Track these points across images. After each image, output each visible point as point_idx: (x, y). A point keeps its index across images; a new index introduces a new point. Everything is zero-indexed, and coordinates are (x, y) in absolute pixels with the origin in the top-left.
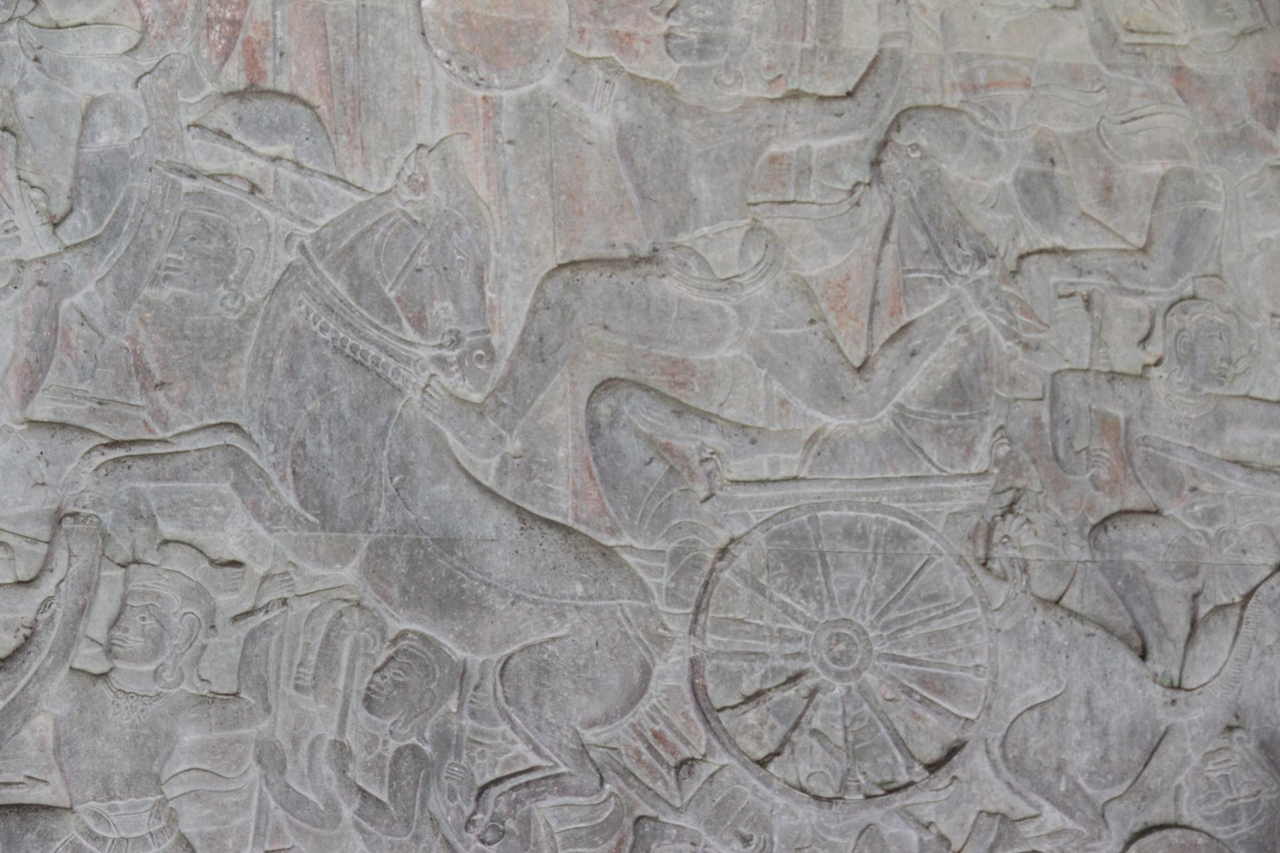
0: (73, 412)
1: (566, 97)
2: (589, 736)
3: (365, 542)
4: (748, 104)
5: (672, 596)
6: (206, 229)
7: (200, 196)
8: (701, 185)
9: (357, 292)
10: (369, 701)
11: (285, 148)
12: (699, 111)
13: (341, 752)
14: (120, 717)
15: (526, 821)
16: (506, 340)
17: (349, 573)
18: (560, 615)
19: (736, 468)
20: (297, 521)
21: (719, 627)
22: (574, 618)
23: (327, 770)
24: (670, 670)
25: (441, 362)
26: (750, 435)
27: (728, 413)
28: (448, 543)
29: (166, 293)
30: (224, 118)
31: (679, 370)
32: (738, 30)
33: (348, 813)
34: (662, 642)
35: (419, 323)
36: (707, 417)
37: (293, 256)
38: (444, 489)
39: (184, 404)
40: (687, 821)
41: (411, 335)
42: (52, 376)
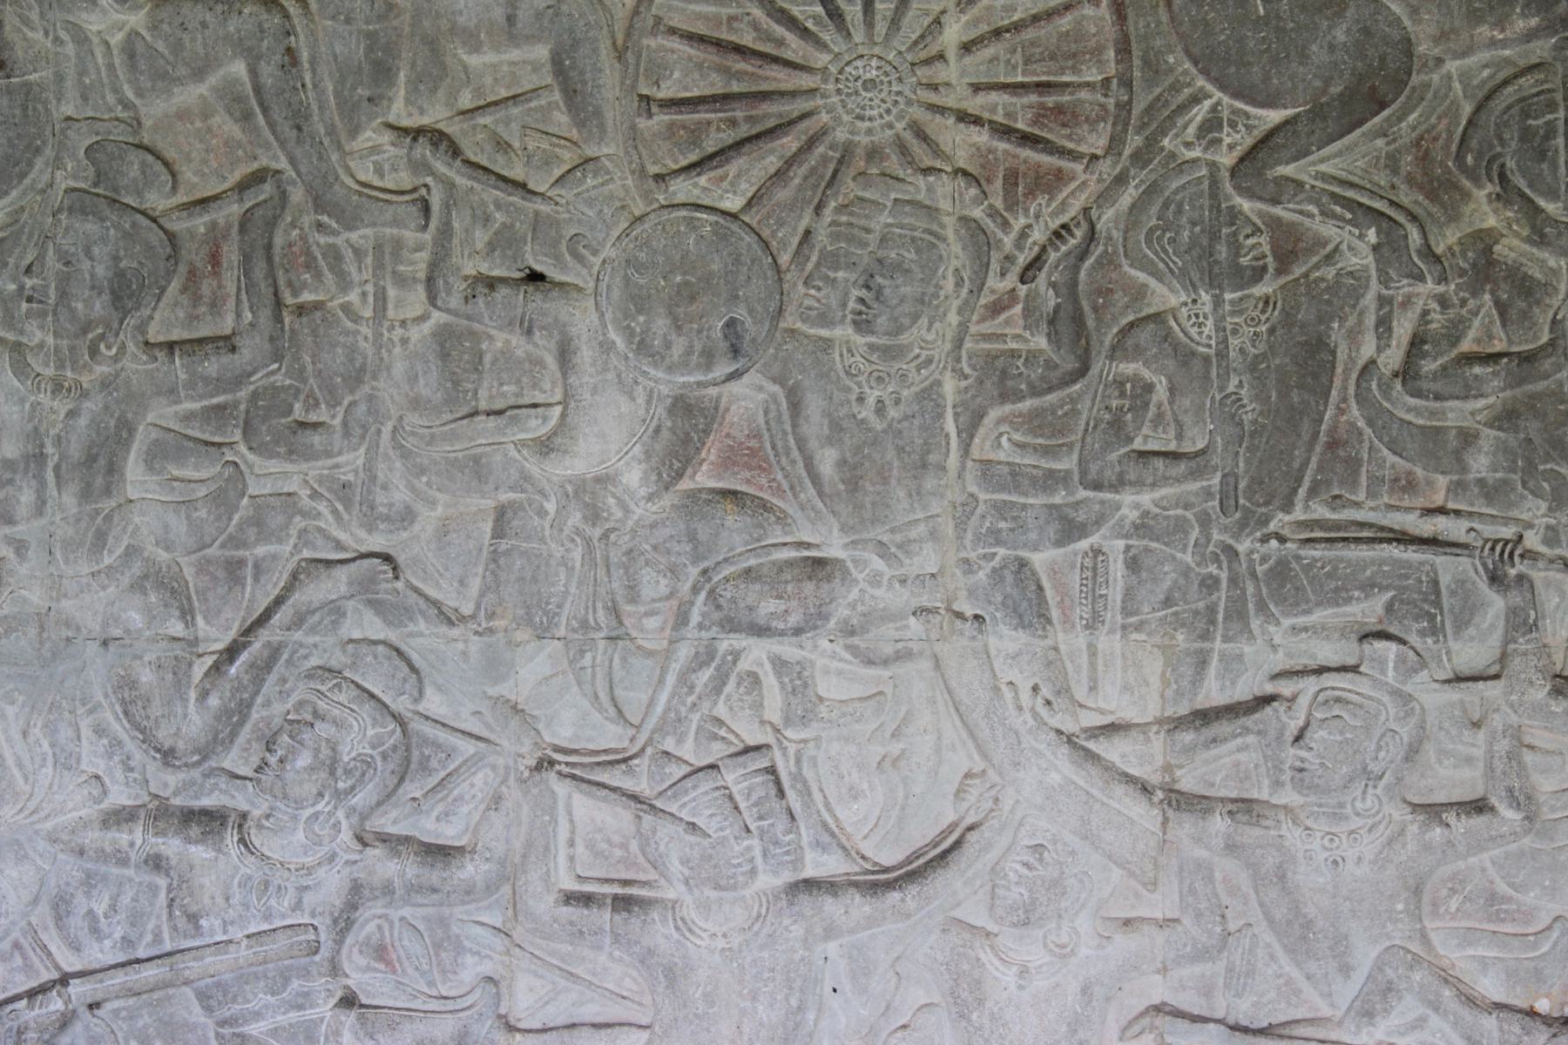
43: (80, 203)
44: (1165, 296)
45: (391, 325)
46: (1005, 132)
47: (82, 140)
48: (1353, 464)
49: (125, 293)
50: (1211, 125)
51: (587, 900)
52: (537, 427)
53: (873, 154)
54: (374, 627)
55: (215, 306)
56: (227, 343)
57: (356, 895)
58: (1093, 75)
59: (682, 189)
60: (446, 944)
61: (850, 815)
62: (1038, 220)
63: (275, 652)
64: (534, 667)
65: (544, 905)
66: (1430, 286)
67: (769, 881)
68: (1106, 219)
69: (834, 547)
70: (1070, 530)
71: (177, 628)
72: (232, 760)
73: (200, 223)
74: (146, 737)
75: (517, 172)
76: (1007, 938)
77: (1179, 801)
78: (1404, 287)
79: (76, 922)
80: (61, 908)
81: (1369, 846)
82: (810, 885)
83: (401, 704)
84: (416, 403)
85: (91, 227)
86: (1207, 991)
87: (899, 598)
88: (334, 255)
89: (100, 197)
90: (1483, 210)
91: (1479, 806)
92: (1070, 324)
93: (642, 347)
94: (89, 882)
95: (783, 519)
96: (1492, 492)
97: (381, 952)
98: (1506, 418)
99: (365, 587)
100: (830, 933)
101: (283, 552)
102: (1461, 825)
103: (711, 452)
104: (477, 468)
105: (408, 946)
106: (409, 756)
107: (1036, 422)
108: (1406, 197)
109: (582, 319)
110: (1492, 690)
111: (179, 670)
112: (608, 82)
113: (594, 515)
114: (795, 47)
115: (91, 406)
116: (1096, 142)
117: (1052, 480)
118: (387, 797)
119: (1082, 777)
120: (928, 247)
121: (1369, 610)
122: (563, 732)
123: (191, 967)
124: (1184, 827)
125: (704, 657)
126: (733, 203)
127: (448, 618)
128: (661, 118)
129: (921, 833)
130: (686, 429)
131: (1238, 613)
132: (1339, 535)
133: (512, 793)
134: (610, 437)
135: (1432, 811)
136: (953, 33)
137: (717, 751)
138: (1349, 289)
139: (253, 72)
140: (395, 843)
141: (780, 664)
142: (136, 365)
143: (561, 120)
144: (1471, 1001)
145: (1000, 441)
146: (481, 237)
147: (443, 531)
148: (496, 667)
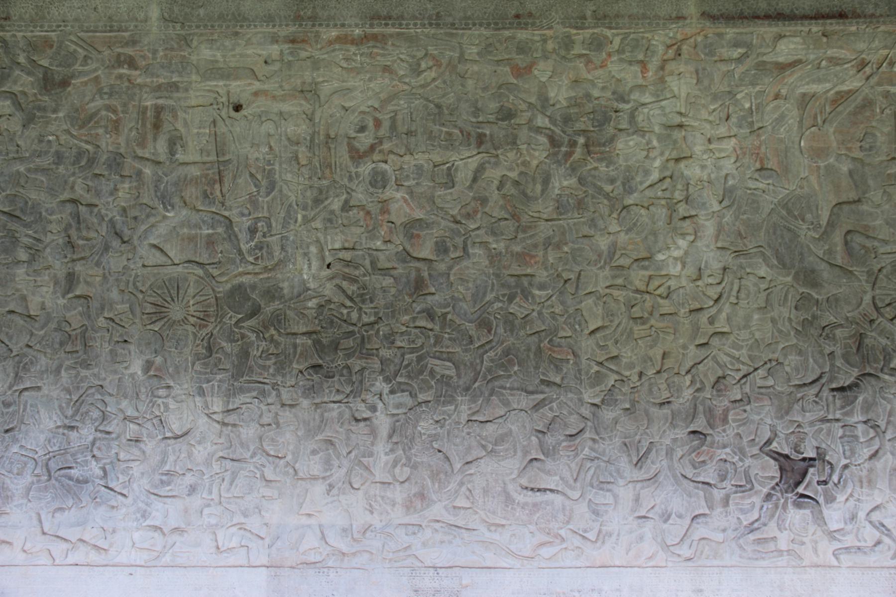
0: (726, 245)
1: (836, 164)
2: (848, 315)
3: (793, 272)
4: (882, 162)
5: (867, 281)
6: (754, 201)
7: (752, 194)
8: (871, 182)
9: (788, 214)
10: (796, 308)
11: (770, 181)
12: (869, 164)
13: (790, 319)
14: (741, 313)
15: (834, 335)
16: (824, 223)
17: (789, 279)
18: (840, 287)
19: (882, 250)
20: (777, 267)
21: (880, 288)
22: (844, 288)
23: (787, 324)
24: (867, 298)
25: (809, 229)
26: (885, 242)
27: (880, 237)
28: (813, 271)
29: (745, 217)
30: (756, 176)
31: (867, 227)
32: (878, 144)
33: (792, 333)
34: (865, 292)
35: (803, 220)
36: (874, 238)
37: (773, 206)
38: (811, 259)
39: (751, 242)
40: (873, 334)
41: (801, 223)
42: (721, 237)
43: (56, 330)
44: (224, 344)
45: (102, 347)
46: (198, 318)
47: (56, 320)
48: (252, 371)
50: (231, 317)
52: (125, 365)
53: (179, 321)
54: (100, 397)
56: (77, 352)
57: (95, 440)
58: (212, 309)
59: (149, 327)
60: (109, 448)
61: (173, 427)
62: (204, 332)
63: (83, 401)
64: (124, 404)
65: (124, 441)
66: (264, 343)
67: (160, 437)
68: (215, 332)
69: (172, 384)
70: (208, 381)
71: (68, 397)
72: (77, 418)
73: (74, 333)
74: (63, 414)
75: (123, 324)
76: (197, 446)
77: (224, 424)
78: (260, 343)
80: (49, 441)
81: (253, 431)
82: (166, 438)
83: (103, 409)
84: (107, 361)
85: (56, 334)
86: (228, 454)
87: (182, 392)
89: (59, 329)
90: (273, 331)
91: (270, 425)
92: (209, 349)
93: (141, 352)
94: (54, 437)
95: (164, 379)
96: (273, 375)
97: (99, 449)
98: (275, 364)
99: (98, 391)
100: (169, 445)
101: (85, 385)
102: (266, 428)
103: (153, 369)
104: (115, 372)
105: (103, 448)
106: (104, 417)
107: (204, 364)
108: (261, 329)
109: (132, 348)
110: (273, 407)
111: (68, 404)
112: (138, 310)
113: (133, 379)
114: (167, 305)
115: (56, 362)
116: (213, 320)
117: (206, 373)
118: (101, 424)
119: (209, 421)
120: (187, 336)
121: (254, 394)
122: (129, 414)
124: (224, 429)
125: (151, 401)
126: (156, 329)
128: (146, 316)
129: (185, 430)
130: (148, 366)
131: (234, 394)
132: (249, 382)
134: (137, 367)
135: (263, 426)
136: (191, 303)
138: (252, 343)
140: (101, 431)
141: (163, 403)
142: (63, 355)
143: (131, 316)
144: (268, 455)
145: (198, 367)
148: (118, 403)
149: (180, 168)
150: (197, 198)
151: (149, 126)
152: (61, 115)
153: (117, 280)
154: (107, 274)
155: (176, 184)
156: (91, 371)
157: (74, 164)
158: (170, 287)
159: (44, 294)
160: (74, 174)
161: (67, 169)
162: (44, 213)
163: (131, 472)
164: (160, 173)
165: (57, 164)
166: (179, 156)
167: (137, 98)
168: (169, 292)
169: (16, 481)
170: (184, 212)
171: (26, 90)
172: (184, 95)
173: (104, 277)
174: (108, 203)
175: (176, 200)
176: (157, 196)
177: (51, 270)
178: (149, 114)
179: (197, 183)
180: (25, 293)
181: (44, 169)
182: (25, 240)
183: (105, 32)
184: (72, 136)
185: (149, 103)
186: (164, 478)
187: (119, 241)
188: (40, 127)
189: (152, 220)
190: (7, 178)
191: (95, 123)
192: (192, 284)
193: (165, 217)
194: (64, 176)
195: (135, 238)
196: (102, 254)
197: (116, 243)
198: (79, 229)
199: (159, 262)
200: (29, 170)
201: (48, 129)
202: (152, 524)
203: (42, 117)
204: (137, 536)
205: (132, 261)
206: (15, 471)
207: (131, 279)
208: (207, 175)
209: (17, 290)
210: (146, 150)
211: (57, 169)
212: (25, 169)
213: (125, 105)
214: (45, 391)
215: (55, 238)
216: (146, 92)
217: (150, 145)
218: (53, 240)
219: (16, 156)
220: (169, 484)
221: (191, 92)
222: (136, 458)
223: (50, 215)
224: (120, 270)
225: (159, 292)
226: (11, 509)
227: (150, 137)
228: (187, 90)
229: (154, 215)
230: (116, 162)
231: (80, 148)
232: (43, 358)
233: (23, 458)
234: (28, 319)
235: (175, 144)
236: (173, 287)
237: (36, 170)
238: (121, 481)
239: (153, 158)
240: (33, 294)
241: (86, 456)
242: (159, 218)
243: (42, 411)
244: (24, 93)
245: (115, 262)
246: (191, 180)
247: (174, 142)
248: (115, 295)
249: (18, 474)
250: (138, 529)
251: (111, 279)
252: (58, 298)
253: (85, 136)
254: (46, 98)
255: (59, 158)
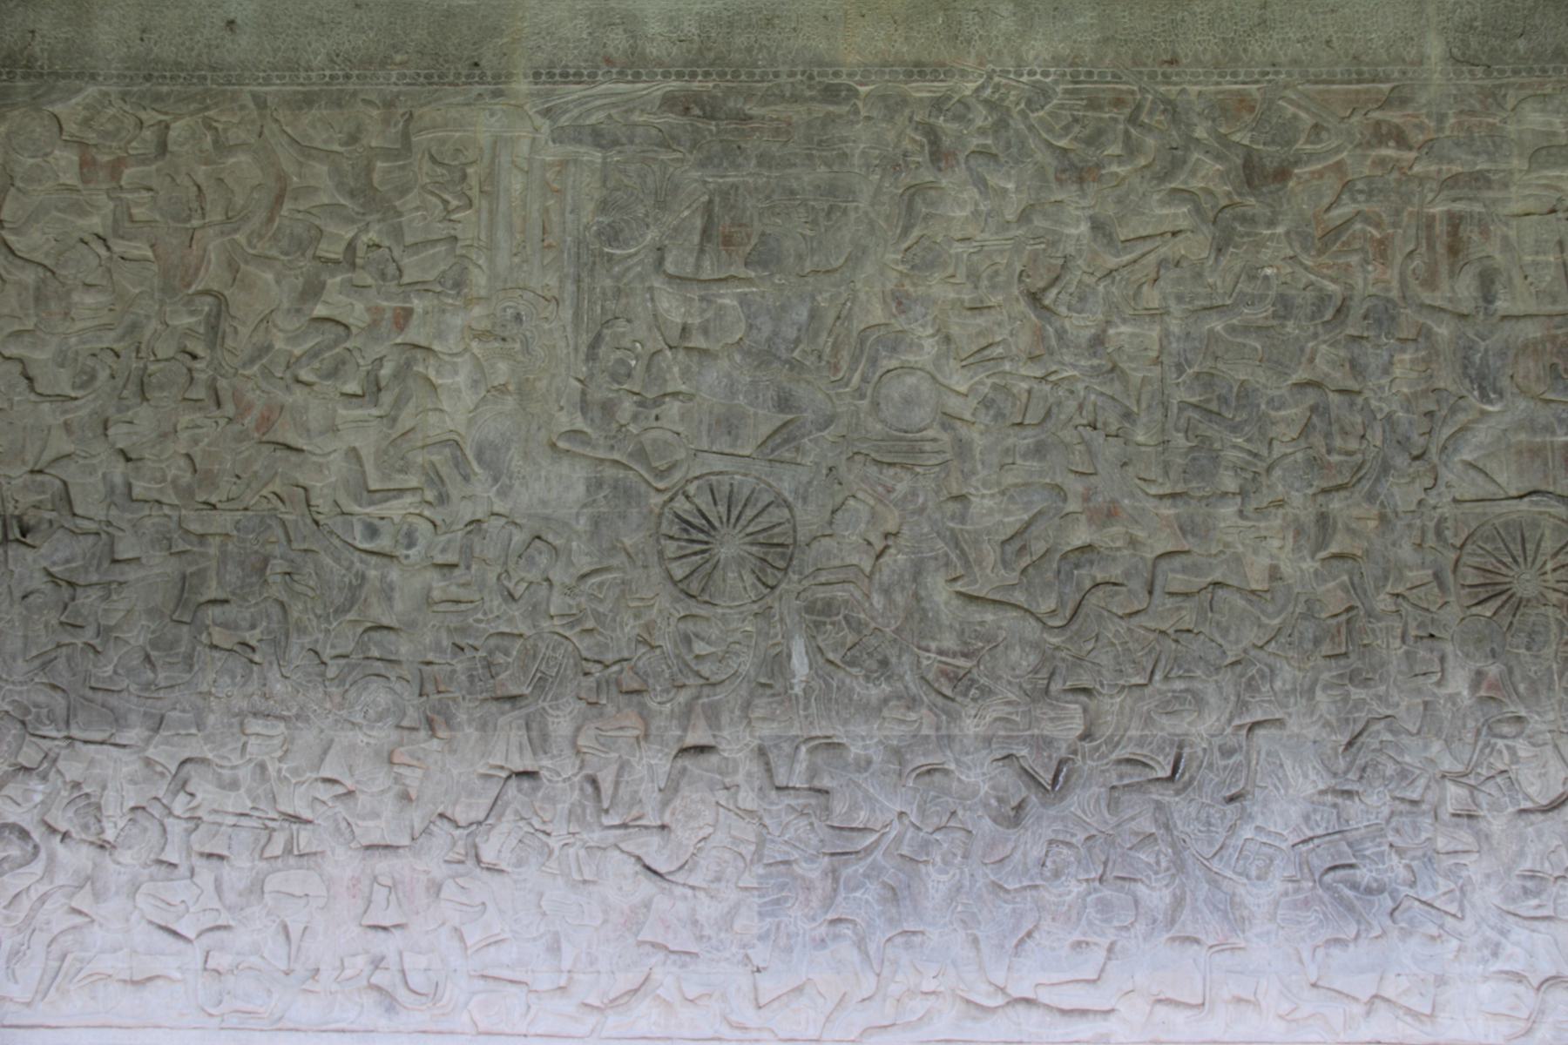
43: (1303, 616)
47: (1302, 599)
49: (1317, 642)
51: (1459, 816)
52: (1435, 678)
53: (1528, 600)
55: (1340, 645)
56: (1345, 655)
57: (1392, 814)
59: (1475, 610)
60: (1417, 829)
61: (1531, 791)
67: (1511, 809)
69: (1523, 713)
74: (1328, 769)
79: (1312, 823)
84: (1400, 672)
87: (1544, 727)
88: (1373, 630)
93: (1467, 655)
94: (1315, 811)
97: (1397, 831)
100: (1532, 824)
101: (1363, 715)
103: (1484, 685)
104: (1419, 691)
112: (1449, 578)
113: (1454, 704)
114: (1504, 570)
120: (1547, 626)
123: (1348, 835)
125: (1487, 744)
127: (1410, 734)
133: (1433, 784)
134: (1459, 683)
136: (1549, 566)
137: (1493, 772)
139: (1351, 579)
140: (1402, 800)
141: (1508, 747)
142: (1321, 662)
143: (1436, 590)
146: (1415, 624)
147: (1408, 709)
148: (1426, 747)
149: (1507, 325)
150: (1538, 378)
151: (1441, 249)
152: (1280, 230)
153: (1409, 526)
154: (1391, 515)
155: (1502, 354)
156: (1372, 691)
157: (1313, 318)
158: (1508, 539)
159: (1275, 551)
160: (1315, 336)
161: (1300, 328)
162: (1263, 407)
163: (1464, 873)
164: (1471, 335)
165: (1285, 318)
166: (1502, 305)
167: (1416, 200)
168: (1507, 548)
169: (1255, 891)
170: (1522, 404)
171: (1211, 186)
172: (1499, 195)
173: (1383, 518)
174: (1381, 388)
175: (1504, 382)
176: (1466, 375)
177: (1288, 509)
178: (1437, 224)
179: (1536, 350)
180: (1240, 549)
181: (1259, 328)
182: (1232, 455)
183: (1350, 82)
184: (1306, 268)
185: (1438, 209)
186: (1529, 884)
187: (1406, 455)
188: (1246, 252)
189: (1462, 418)
190: (1197, 344)
191: (1344, 244)
192: (1547, 532)
193: (1483, 413)
194: (1297, 338)
195: (1433, 450)
196: (1377, 480)
197: (1401, 461)
198: (1328, 435)
199: (1481, 494)
200: (1232, 330)
201: (1261, 256)
202: (1507, 968)
203: (1248, 234)
204: (1485, 990)
205: (1434, 492)
206: (1254, 873)
207: (1432, 524)
208: (1555, 337)
209: (1227, 545)
210: (1437, 294)
211: (1283, 326)
212: (1225, 329)
213: (1398, 212)
214: (1293, 726)
215: (1289, 451)
216: (1431, 190)
217: (1445, 284)
218: (1285, 455)
219: (1206, 303)
220: (1537, 894)
221: (1513, 189)
222: (1466, 848)
223: (1278, 409)
224: (1413, 507)
225: (1488, 547)
226: (1247, 940)
227: (1444, 269)
228: (1506, 186)
229: (1465, 410)
230: (1383, 316)
231: (1321, 290)
232: (1287, 667)
233: (1265, 849)
234: (1254, 598)
235: (1493, 282)
236: (1514, 539)
237: (1246, 329)
238: (1442, 889)
239: (1449, 307)
240: (1256, 552)
241: (1380, 845)
242: (1472, 415)
243: (1288, 764)
244: (1210, 193)
245: (1402, 493)
246: (1526, 346)
247: (1487, 282)
248: (1406, 552)
249: (1259, 878)
250: (1486, 979)
251: (1400, 524)
252: (1303, 559)
253: (1329, 267)
254: (1252, 200)
255: (1285, 307)
